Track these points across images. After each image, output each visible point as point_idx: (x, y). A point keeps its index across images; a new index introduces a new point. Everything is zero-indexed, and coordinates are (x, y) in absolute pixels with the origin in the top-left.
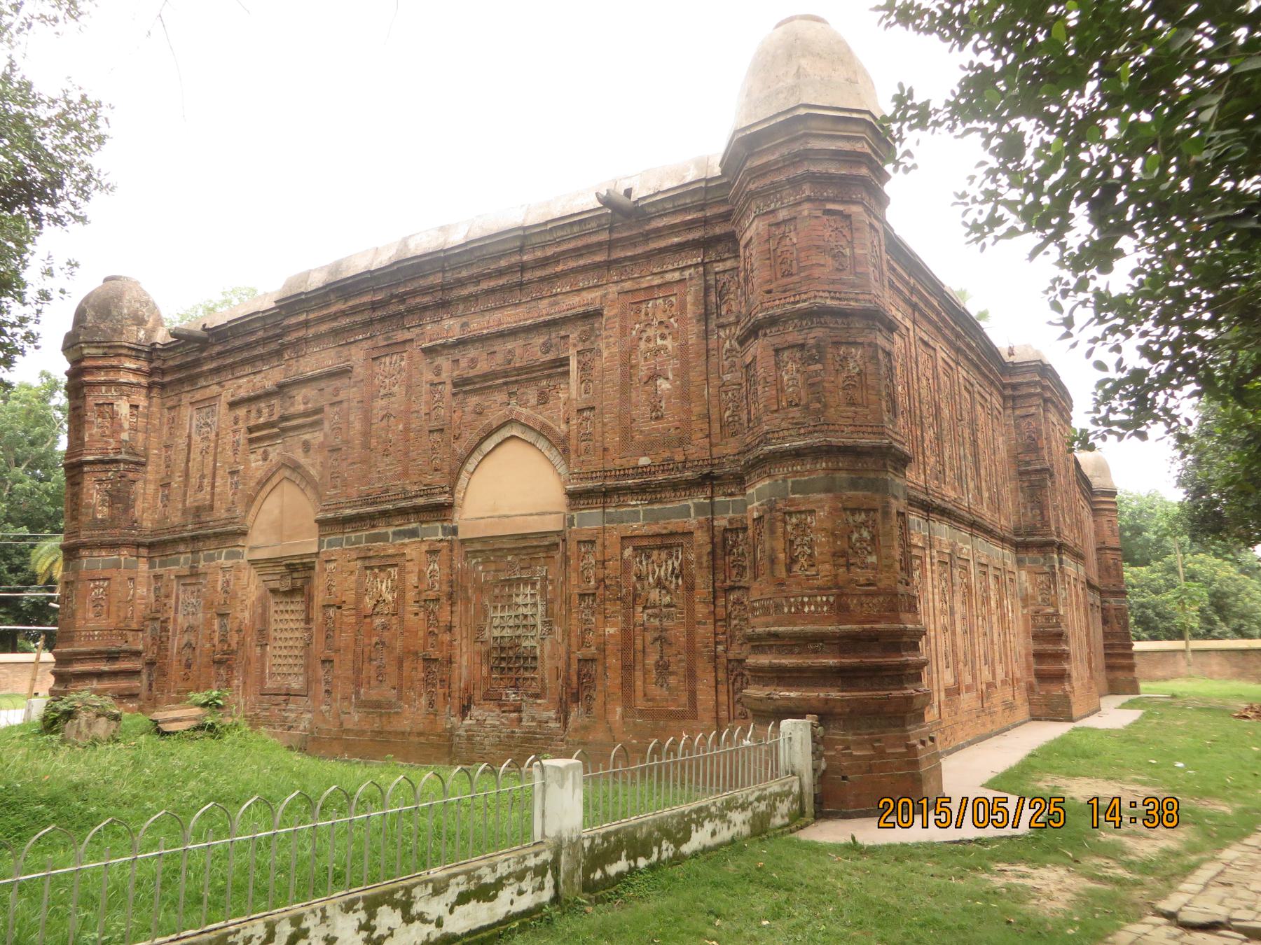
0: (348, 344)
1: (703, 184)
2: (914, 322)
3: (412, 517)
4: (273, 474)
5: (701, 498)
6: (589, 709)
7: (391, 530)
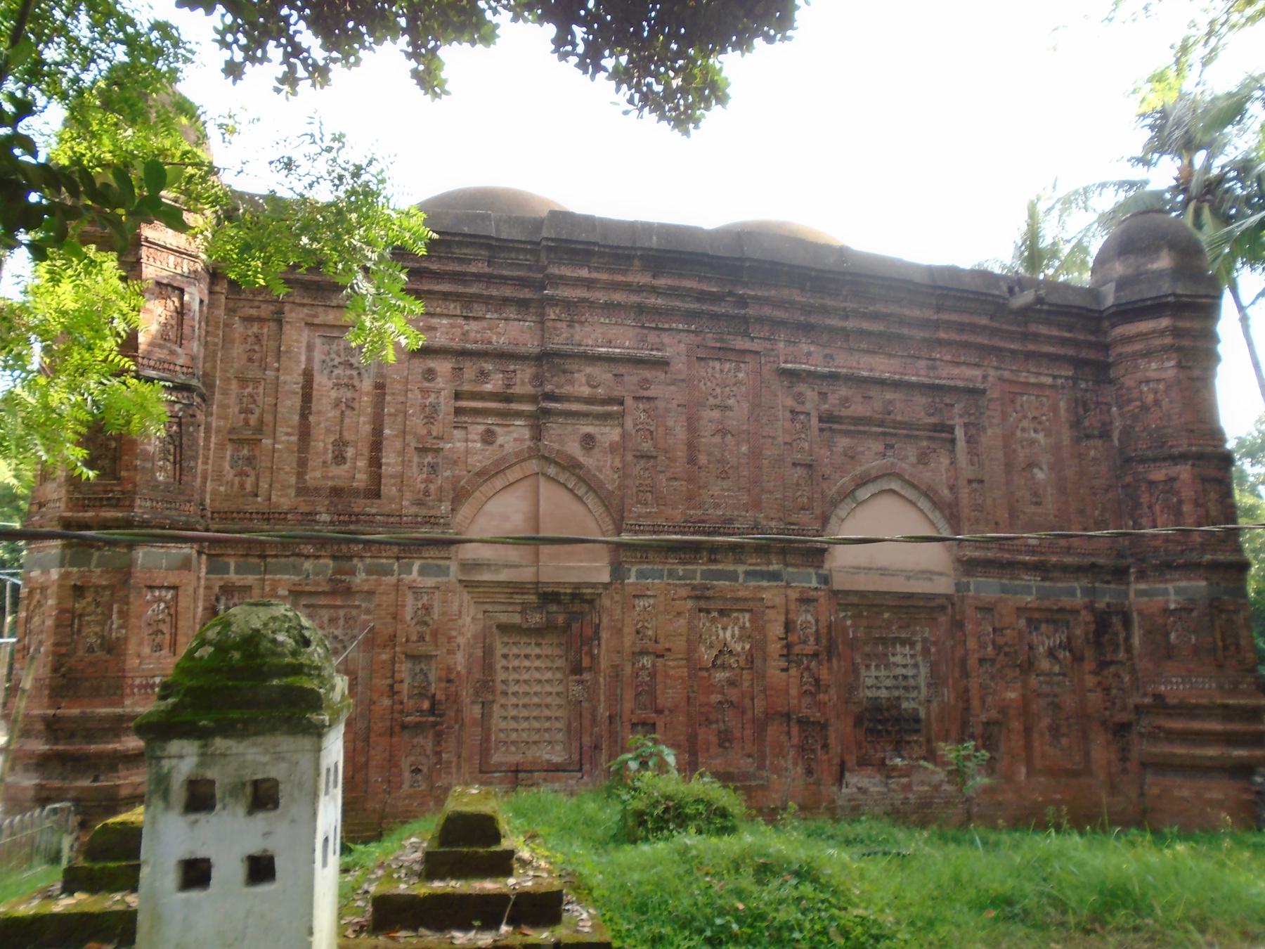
0: (657, 329)
5: (1085, 582)
7: (741, 569)
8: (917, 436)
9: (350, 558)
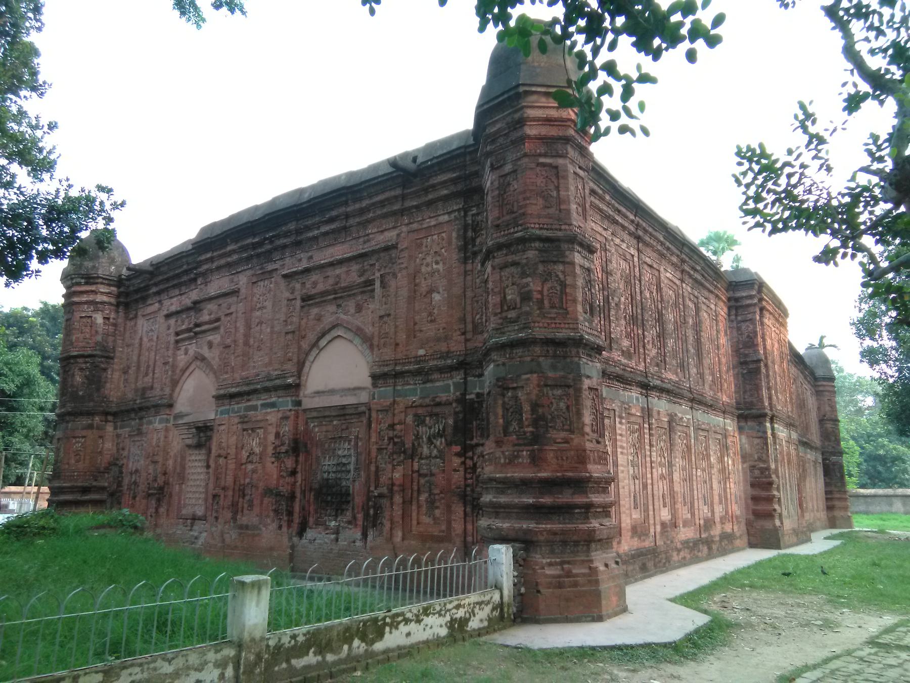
1: (462, 150)
2: (638, 250)
3: (273, 393)
4: (190, 364)
6: (381, 534)
7: (260, 403)
8: (354, 294)
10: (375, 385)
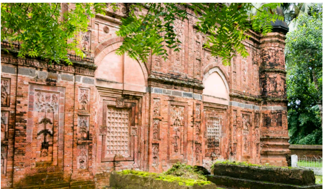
7: (183, 92)
9: (55, 72)
10: (231, 100)
